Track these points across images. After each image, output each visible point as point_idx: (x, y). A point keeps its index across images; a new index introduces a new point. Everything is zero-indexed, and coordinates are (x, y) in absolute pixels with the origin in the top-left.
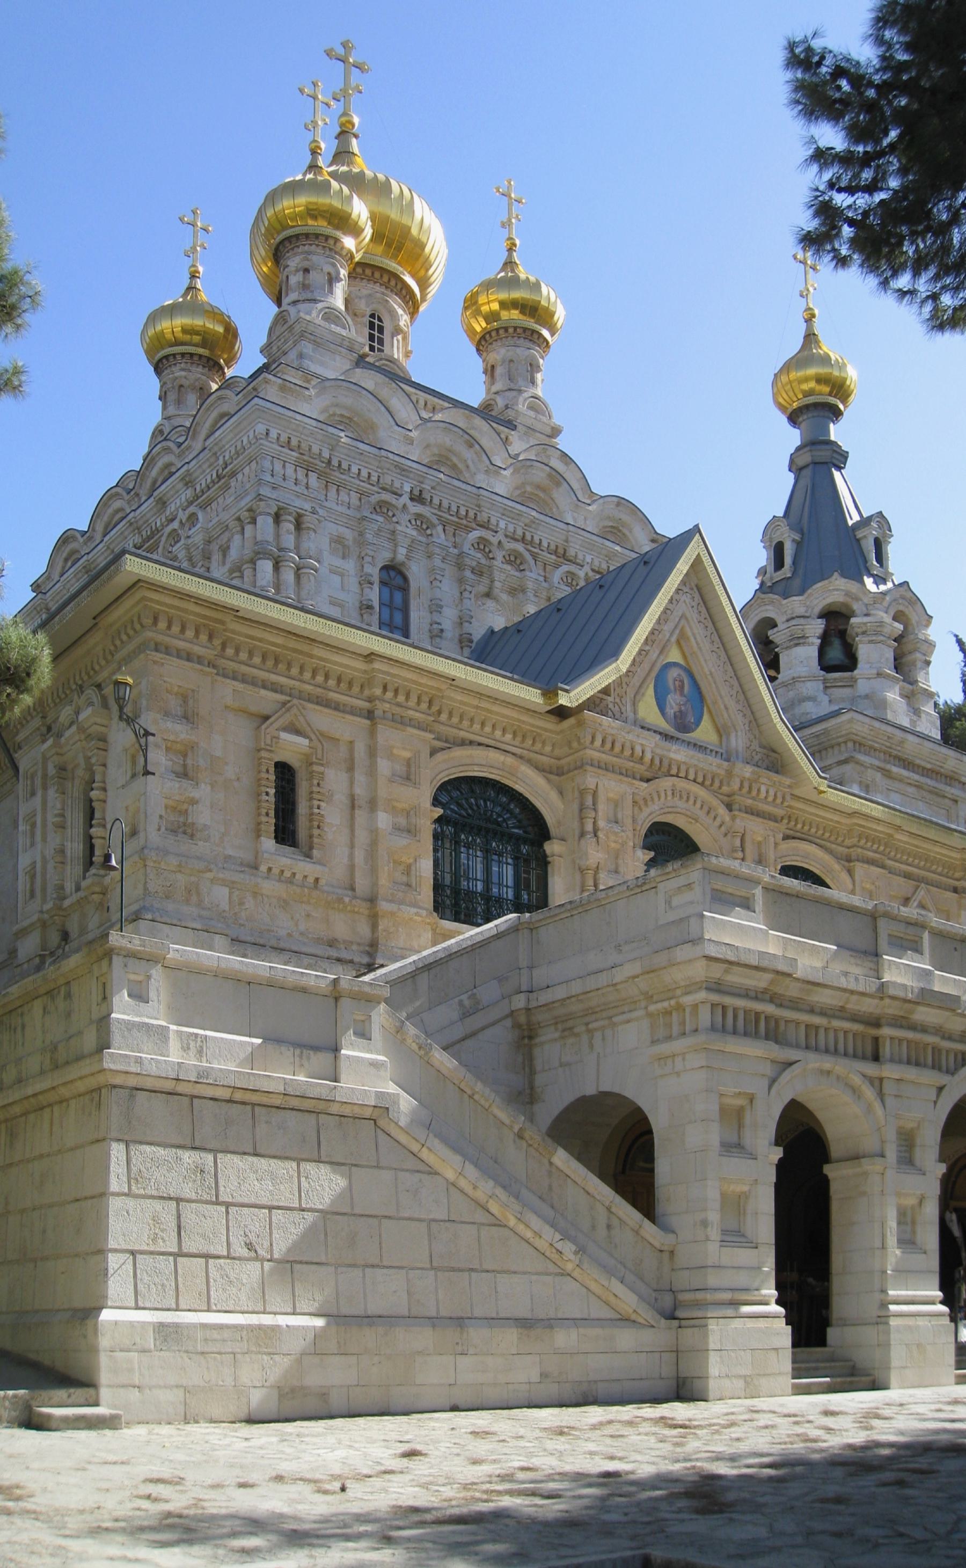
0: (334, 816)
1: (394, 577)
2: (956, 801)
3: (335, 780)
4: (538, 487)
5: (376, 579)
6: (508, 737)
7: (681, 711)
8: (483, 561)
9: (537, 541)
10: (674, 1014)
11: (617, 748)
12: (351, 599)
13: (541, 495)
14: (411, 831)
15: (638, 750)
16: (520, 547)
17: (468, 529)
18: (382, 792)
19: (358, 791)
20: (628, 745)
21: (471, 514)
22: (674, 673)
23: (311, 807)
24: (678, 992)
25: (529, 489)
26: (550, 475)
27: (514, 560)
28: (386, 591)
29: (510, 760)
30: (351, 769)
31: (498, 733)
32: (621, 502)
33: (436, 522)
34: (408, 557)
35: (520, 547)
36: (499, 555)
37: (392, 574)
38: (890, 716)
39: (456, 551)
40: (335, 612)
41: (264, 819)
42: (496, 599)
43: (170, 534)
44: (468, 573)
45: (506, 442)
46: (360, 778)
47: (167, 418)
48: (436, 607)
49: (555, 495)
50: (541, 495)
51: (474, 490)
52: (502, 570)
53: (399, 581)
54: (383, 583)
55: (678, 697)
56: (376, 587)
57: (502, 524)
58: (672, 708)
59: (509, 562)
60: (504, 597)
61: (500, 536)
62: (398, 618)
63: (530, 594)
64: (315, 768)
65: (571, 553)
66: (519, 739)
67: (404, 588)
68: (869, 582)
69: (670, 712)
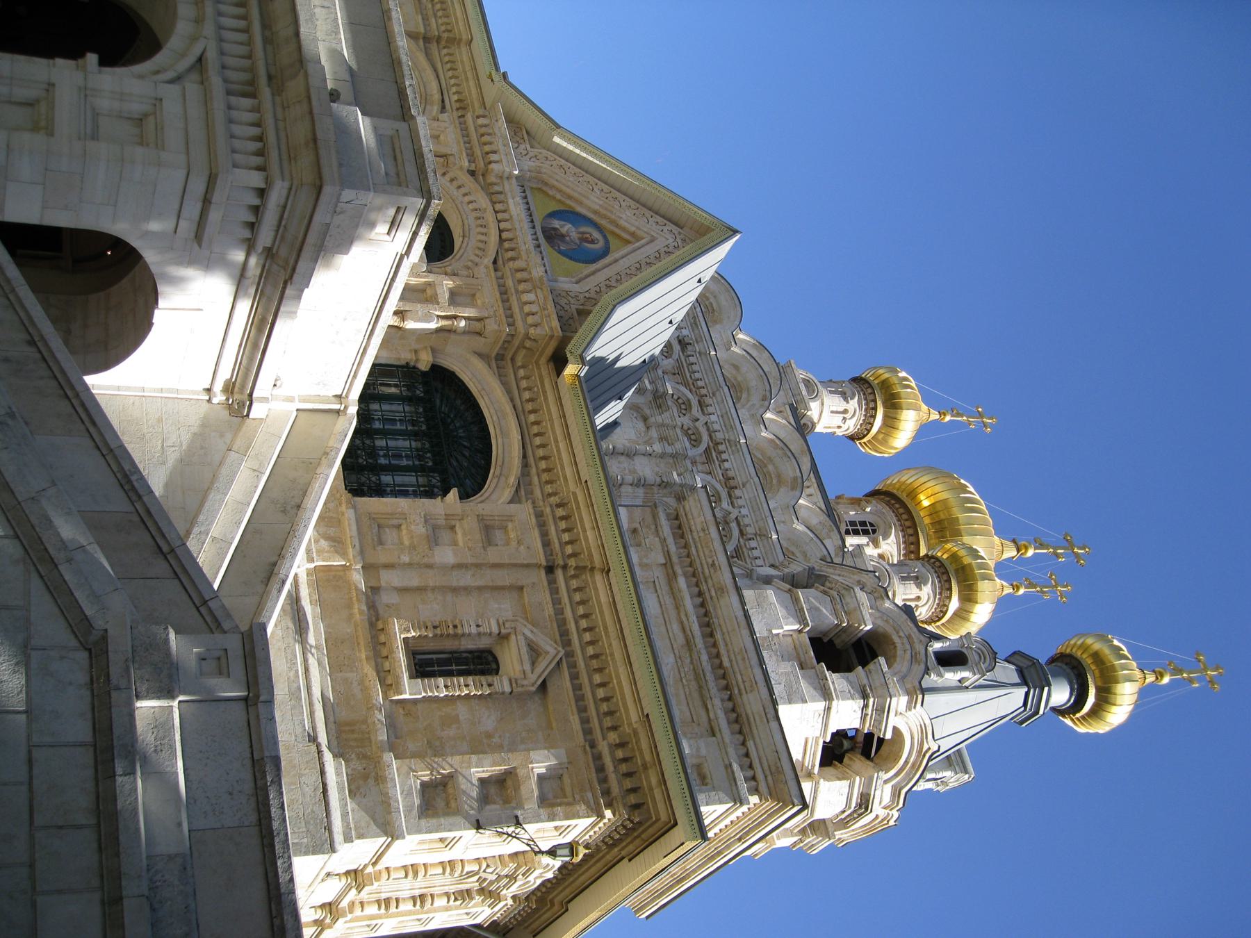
4: (779, 476)
6: (455, 97)
7: (563, 236)
9: (724, 456)
11: (486, 139)
13: (775, 481)
20: (493, 147)
22: (596, 235)
25: (770, 467)
26: (795, 479)
29: (437, 97)
31: (454, 89)
35: (705, 438)
50: (775, 481)
55: (574, 235)
58: (562, 226)
60: (654, 433)
61: (703, 419)
65: (737, 492)
66: (458, 105)
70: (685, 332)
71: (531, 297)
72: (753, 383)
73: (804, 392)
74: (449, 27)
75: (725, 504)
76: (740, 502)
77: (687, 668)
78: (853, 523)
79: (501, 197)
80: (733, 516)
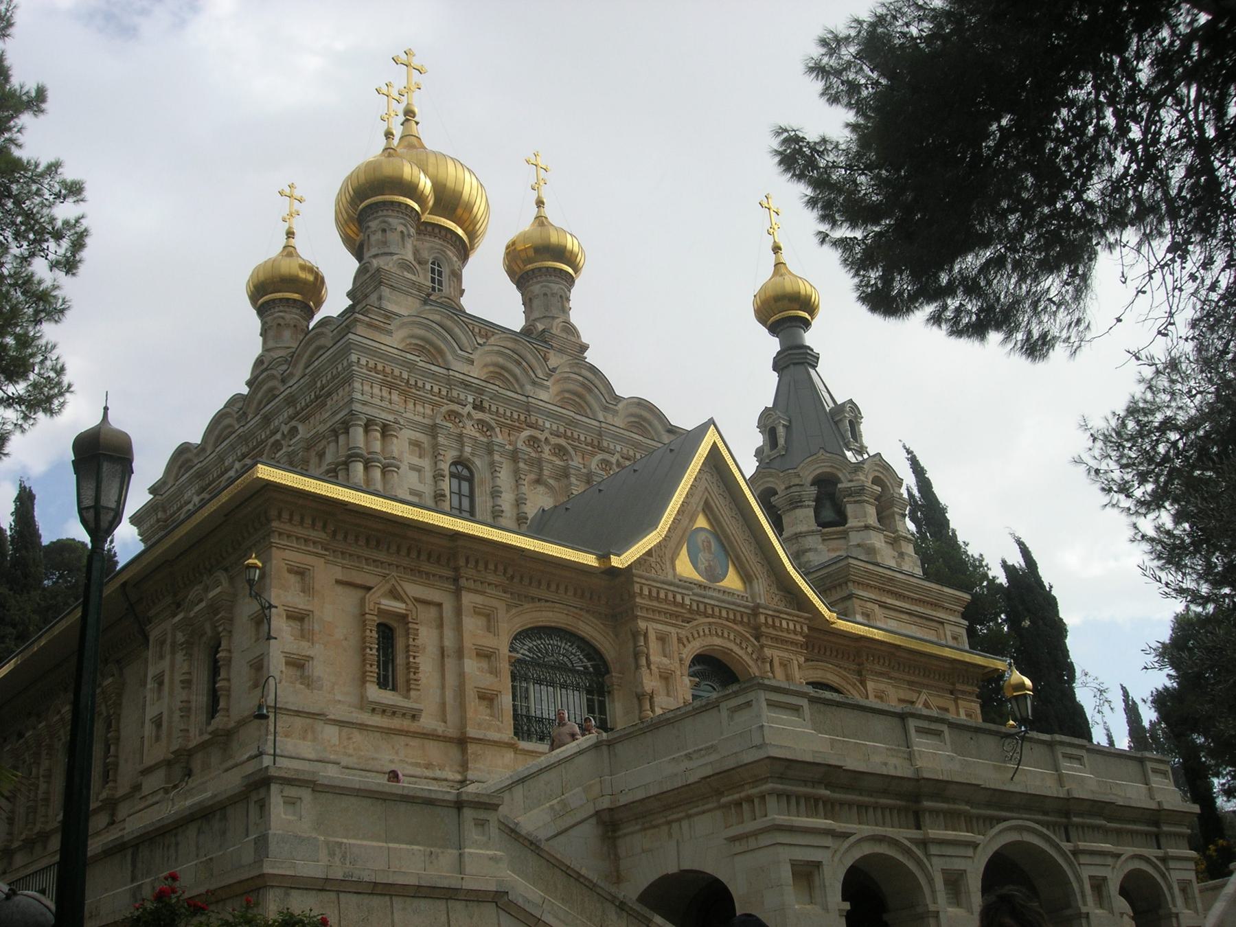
0: (426, 665)
1: (463, 470)
2: (942, 623)
3: (426, 636)
5: (447, 473)
7: (710, 566)
8: (533, 455)
10: (745, 806)
12: (427, 489)
14: (494, 672)
15: (679, 598)
16: (562, 441)
17: (520, 430)
18: (468, 644)
19: (447, 643)
21: (522, 418)
22: (702, 536)
23: (408, 657)
24: (747, 787)
25: (567, 395)
27: (560, 451)
28: (455, 482)
30: (441, 626)
32: (641, 403)
33: (493, 423)
34: (473, 454)
35: (562, 441)
36: (547, 449)
37: (460, 468)
38: (879, 561)
39: (511, 448)
40: (415, 499)
41: (368, 668)
42: (547, 485)
43: (273, 445)
44: (521, 465)
45: (546, 359)
46: (449, 634)
47: (266, 349)
48: (495, 493)
49: (589, 397)
51: (524, 399)
52: (551, 462)
53: (465, 473)
54: (452, 475)
56: (447, 479)
57: (547, 425)
59: (555, 454)
60: (551, 481)
61: (546, 434)
62: (466, 503)
63: (573, 480)
64: (411, 625)
65: (605, 444)
67: (470, 480)
68: (849, 454)
69: (702, 567)
70: (470, 399)
71: (784, 624)
72: (501, 360)
73: (414, 278)
74: (501, 568)
75: (613, 460)
76: (612, 447)
77: (918, 620)
78: (433, 280)
79: (702, 607)
80: (621, 460)
